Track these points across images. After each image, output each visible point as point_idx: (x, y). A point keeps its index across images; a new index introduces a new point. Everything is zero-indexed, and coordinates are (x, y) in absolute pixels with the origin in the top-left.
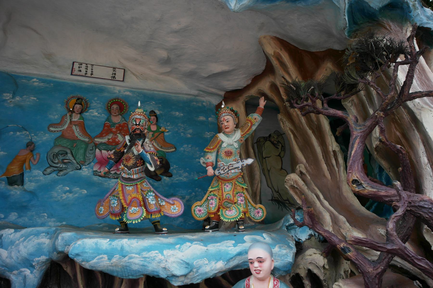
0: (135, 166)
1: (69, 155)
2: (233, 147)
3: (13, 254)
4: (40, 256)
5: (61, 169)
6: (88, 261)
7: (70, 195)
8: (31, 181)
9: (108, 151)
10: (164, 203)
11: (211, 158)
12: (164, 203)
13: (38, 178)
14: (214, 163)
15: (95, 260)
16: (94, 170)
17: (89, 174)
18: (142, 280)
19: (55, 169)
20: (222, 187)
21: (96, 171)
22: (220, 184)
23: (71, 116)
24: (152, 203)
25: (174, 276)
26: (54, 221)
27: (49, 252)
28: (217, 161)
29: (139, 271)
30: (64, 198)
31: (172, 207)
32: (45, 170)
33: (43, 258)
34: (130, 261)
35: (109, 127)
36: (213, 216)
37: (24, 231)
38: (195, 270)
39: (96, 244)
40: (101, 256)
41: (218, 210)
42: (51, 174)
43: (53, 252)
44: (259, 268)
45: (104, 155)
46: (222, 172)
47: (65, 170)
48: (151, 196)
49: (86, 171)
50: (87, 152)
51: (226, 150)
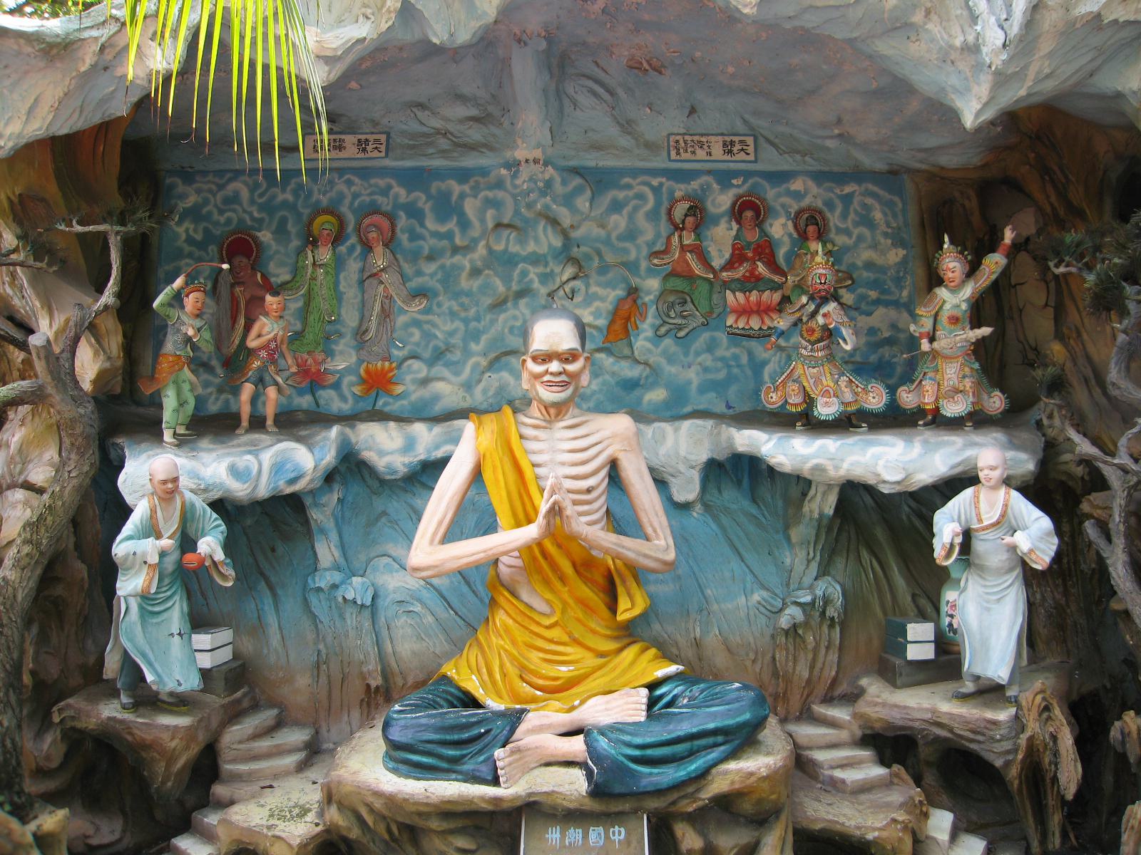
19: (672, 326)
23: (680, 237)
25: (884, 482)
28: (934, 329)
35: (743, 248)
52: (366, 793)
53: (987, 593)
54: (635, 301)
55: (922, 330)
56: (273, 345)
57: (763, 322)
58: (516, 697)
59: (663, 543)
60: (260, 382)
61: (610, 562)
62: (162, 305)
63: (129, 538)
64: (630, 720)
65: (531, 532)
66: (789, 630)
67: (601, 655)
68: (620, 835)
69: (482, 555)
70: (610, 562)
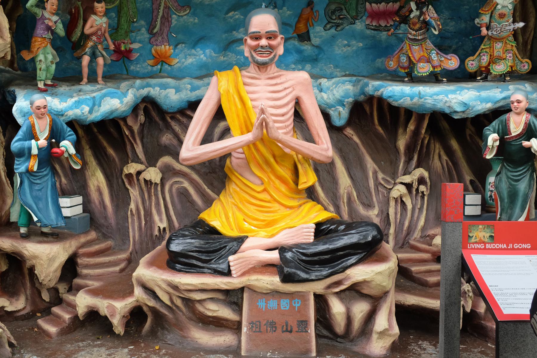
0: (420, 29)
1: (344, 12)
2: (507, 8)
3: (330, 96)
4: (348, 98)
5: (339, 24)
6: (397, 101)
7: (349, 48)
8: (315, 37)
9: (377, 4)
10: (443, 59)
11: (486, 19)
12: (443, 59)
13: (321, 34)
14: (488, 24)
15: (402, 101)
16: (367, 23)
17: (362, 28)
18: (428, 115)
19: (333, 24)
20: (493, 45)
21: (369, 25)
22: (492, 42)
24: (434, 59)
25: (456, 112)
26: (339, 72)
27: (355, 96)
28: (490, 22)
29: (430, 109)
30: (344, 51)
31: (450, 62)
32: (325, 26)
33: (351, 100)
34: (425, 101)
36: (484, 69)
37: (334, 80)
38: (470, 108)
39: (402, 90)
40: (405, 98)
41: (489, 65)
42: (331, 30)
43: (360, 95)
44: (517, 107)
45: (374, 9)
46: (495, 33)
47: (342, 25)
48: (434, 53)
49: (359, 26)
50: (359, 6)
51: (500, 12)
52: (158, 280)
53: (513, 176)
54: (312, 9)
55: (483, 22)
56: (99, 33)
57: (388, 23)
58: (240, 229)
59: (325, 146)
60: (94, 56)
61: (295, 156)
62: (32, 6)
63: (19, 140)
64: (304, 241)
65: (249, 137)
66: (397, 198)
67: (291, 208)
68: (298, 303)
69: (222, 151)
70: (295, 156)
